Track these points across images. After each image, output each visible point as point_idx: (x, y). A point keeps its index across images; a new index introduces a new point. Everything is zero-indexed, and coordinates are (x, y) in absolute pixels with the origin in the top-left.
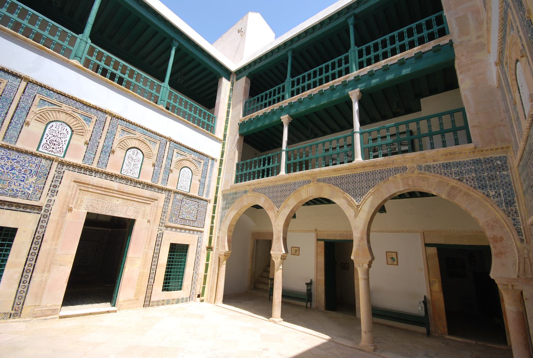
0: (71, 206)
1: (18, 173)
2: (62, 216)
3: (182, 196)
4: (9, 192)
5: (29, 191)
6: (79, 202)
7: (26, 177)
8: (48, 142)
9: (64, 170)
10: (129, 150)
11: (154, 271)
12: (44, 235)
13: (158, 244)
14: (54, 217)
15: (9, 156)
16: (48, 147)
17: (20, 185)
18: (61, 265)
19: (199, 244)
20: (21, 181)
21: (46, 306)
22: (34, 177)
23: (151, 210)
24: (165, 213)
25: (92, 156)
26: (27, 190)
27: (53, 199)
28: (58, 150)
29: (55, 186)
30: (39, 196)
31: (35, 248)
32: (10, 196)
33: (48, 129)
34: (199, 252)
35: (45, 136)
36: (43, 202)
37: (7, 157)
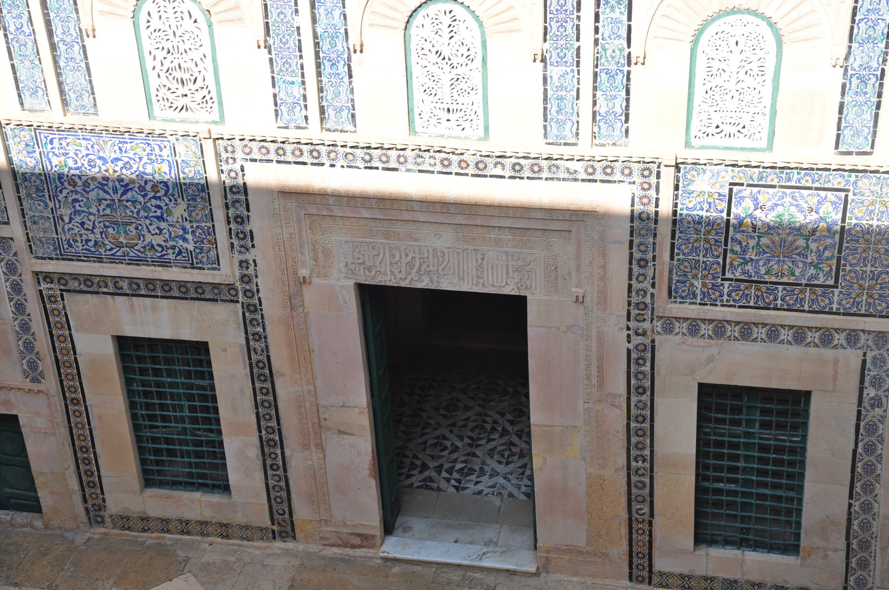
0: (303, 272)
1: (141, 199)
2: (293, 301)
3: (729, 175)
4: (149, 254)
5: (185, 245)
6: (321, 256)
7: (163, 205)
8: (164, 81)
9: (240, 162)
10: (418, 19)
11: (647, 480)
12: (268, 357)
13: (642, 386)
14: (272, 307)
15: (101, 154)
16: (171, 97)
17: (161, 230)
18: (341, 432)
19: (870, 392)
20: (157, 218)
21: (345, 525)
22: (180, 200)
23: (578, 256)
24: (643, 263)
25: (297, 91)
26: (181, 242)
27: (249, 257)
28: (198, 97)
29: (240, 220)
30: (212, 254)
31: (264, 391)
32: (154, 263)
33: (144, 33)
34: (872, 429)
35: (149, 60)
36: (228, 272)
37: (100, 158)
